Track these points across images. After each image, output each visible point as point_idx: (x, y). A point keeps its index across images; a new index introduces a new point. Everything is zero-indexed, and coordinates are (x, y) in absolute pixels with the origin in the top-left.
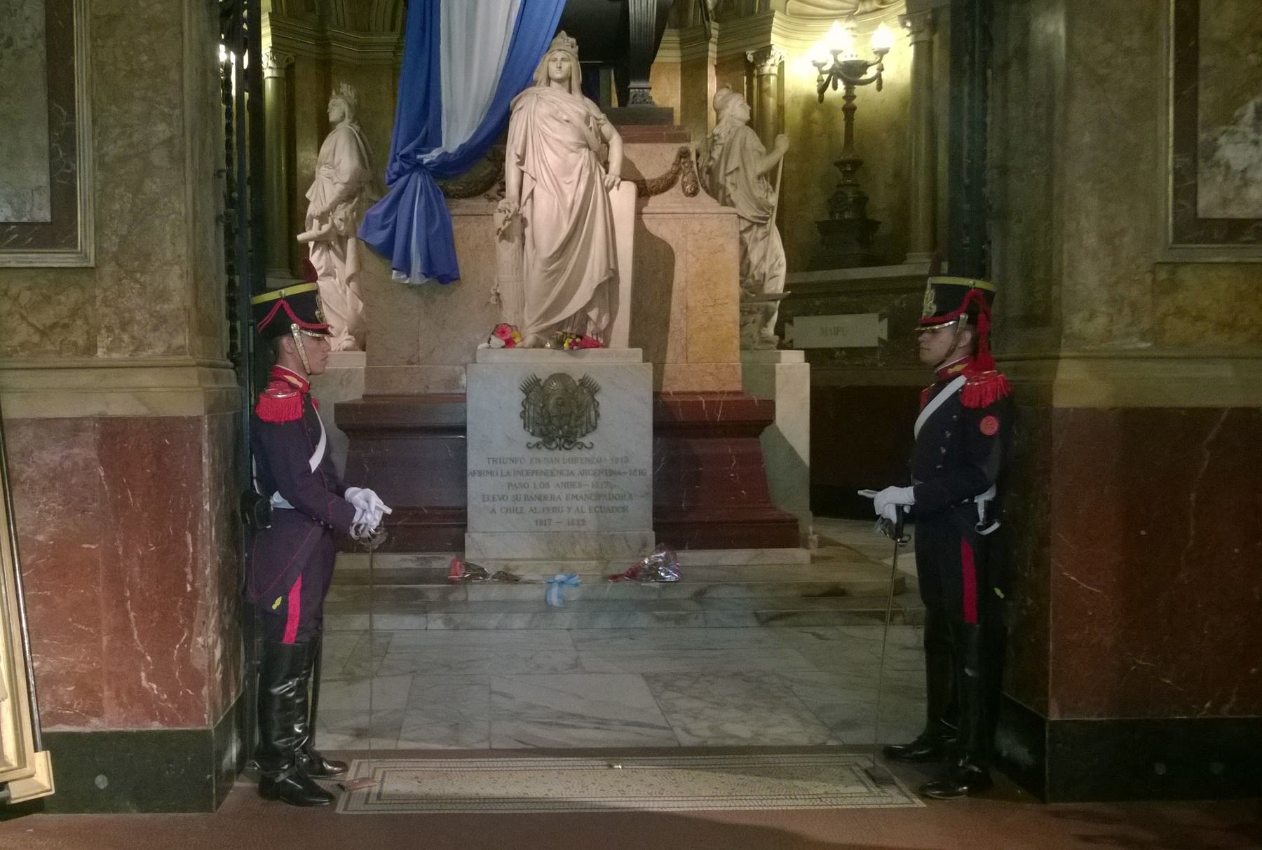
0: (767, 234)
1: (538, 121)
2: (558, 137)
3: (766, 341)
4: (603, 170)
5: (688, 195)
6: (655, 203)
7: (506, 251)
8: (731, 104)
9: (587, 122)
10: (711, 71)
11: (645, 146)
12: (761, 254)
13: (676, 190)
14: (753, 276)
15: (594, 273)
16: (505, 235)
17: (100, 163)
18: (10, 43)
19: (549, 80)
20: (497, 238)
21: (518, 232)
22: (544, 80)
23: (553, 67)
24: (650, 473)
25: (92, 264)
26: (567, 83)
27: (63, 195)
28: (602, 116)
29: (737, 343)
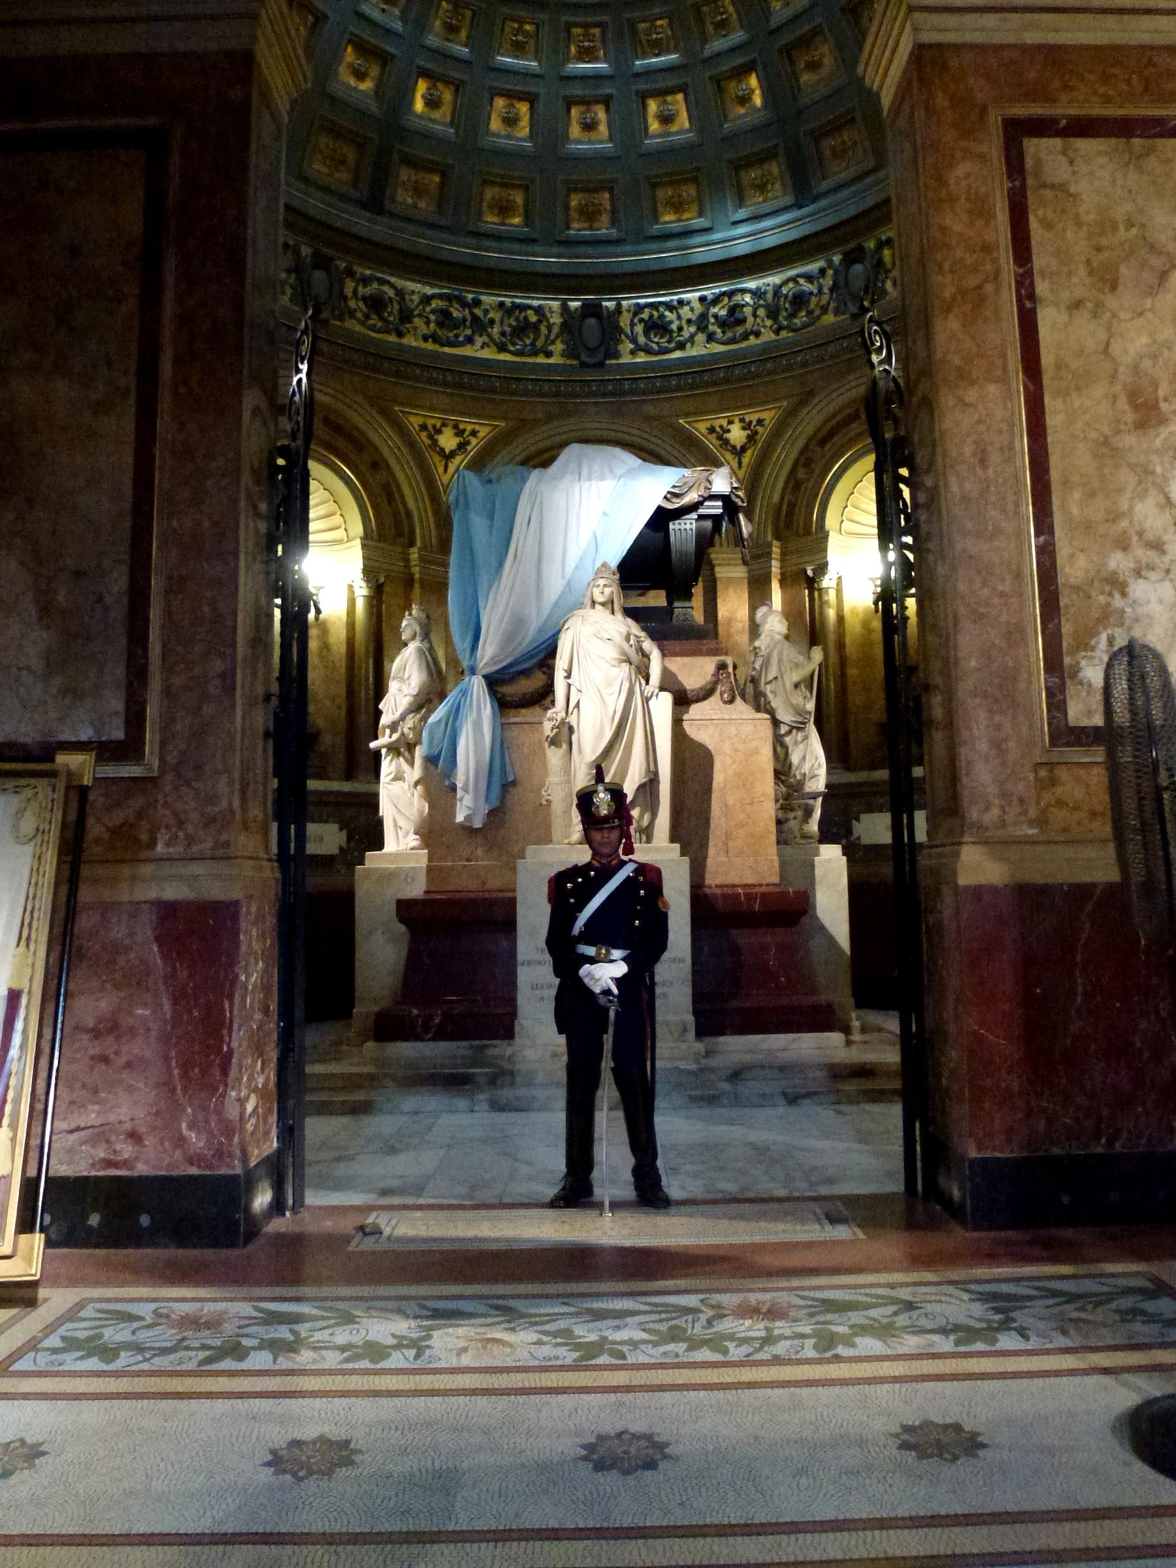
0: (806, 738)
1: (583, 640)
3: (805, 836)
4: (643, 682)
5: (725, 703)
6: (696, 711)
7: (554, 756)
8: (770, 619)
9: (628, 639)
10: (775, 586)
11: (686, 660)
12: (801, 755)
13: (715, 699)
14: (795, 776)
16: (554, 742)
17: (167, 692)
18: (100, 599)
19: (593, 603)
20: (546, 744)
22: (589, 604)
23: (596, 592)
24: (689, 961)
25: (156, 774)
27: (135, 719)
28: (643, 634)
29: (773, 838)
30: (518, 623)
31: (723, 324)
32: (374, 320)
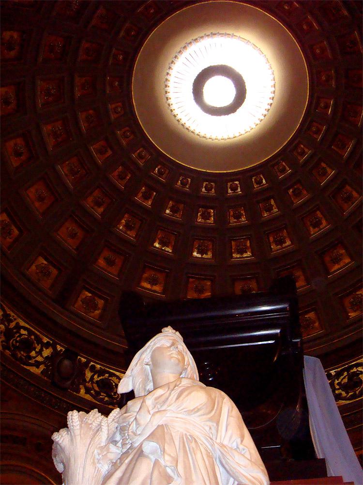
31: (343, 387)
32: (103, 395)
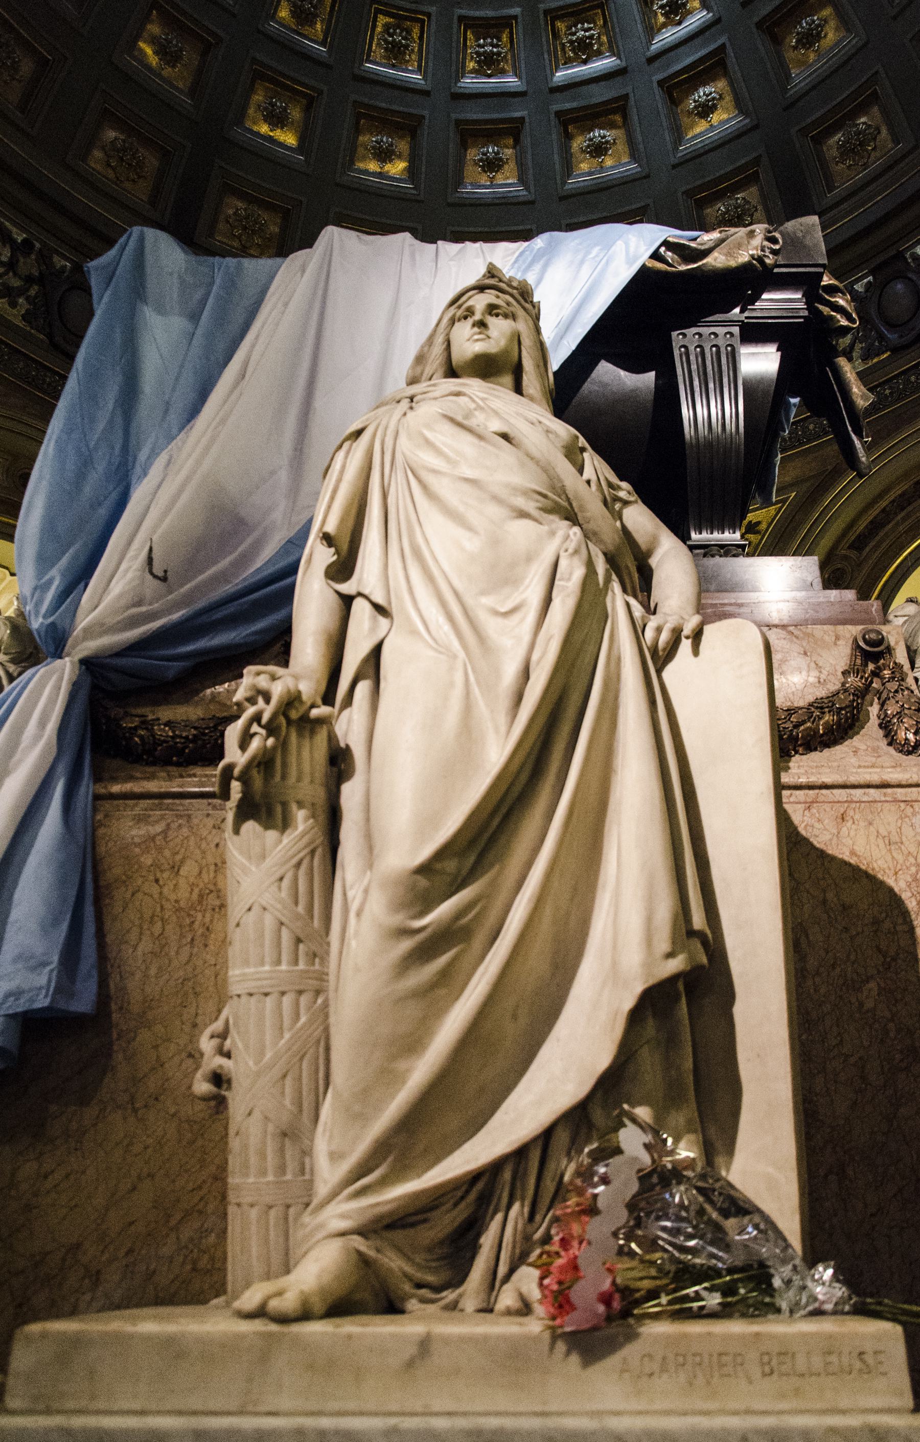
2: (469, 473)
7: (256, 866)
15: (623, 948)
21: (319, 794)
26: (508, 379)
30: (223, 524)
